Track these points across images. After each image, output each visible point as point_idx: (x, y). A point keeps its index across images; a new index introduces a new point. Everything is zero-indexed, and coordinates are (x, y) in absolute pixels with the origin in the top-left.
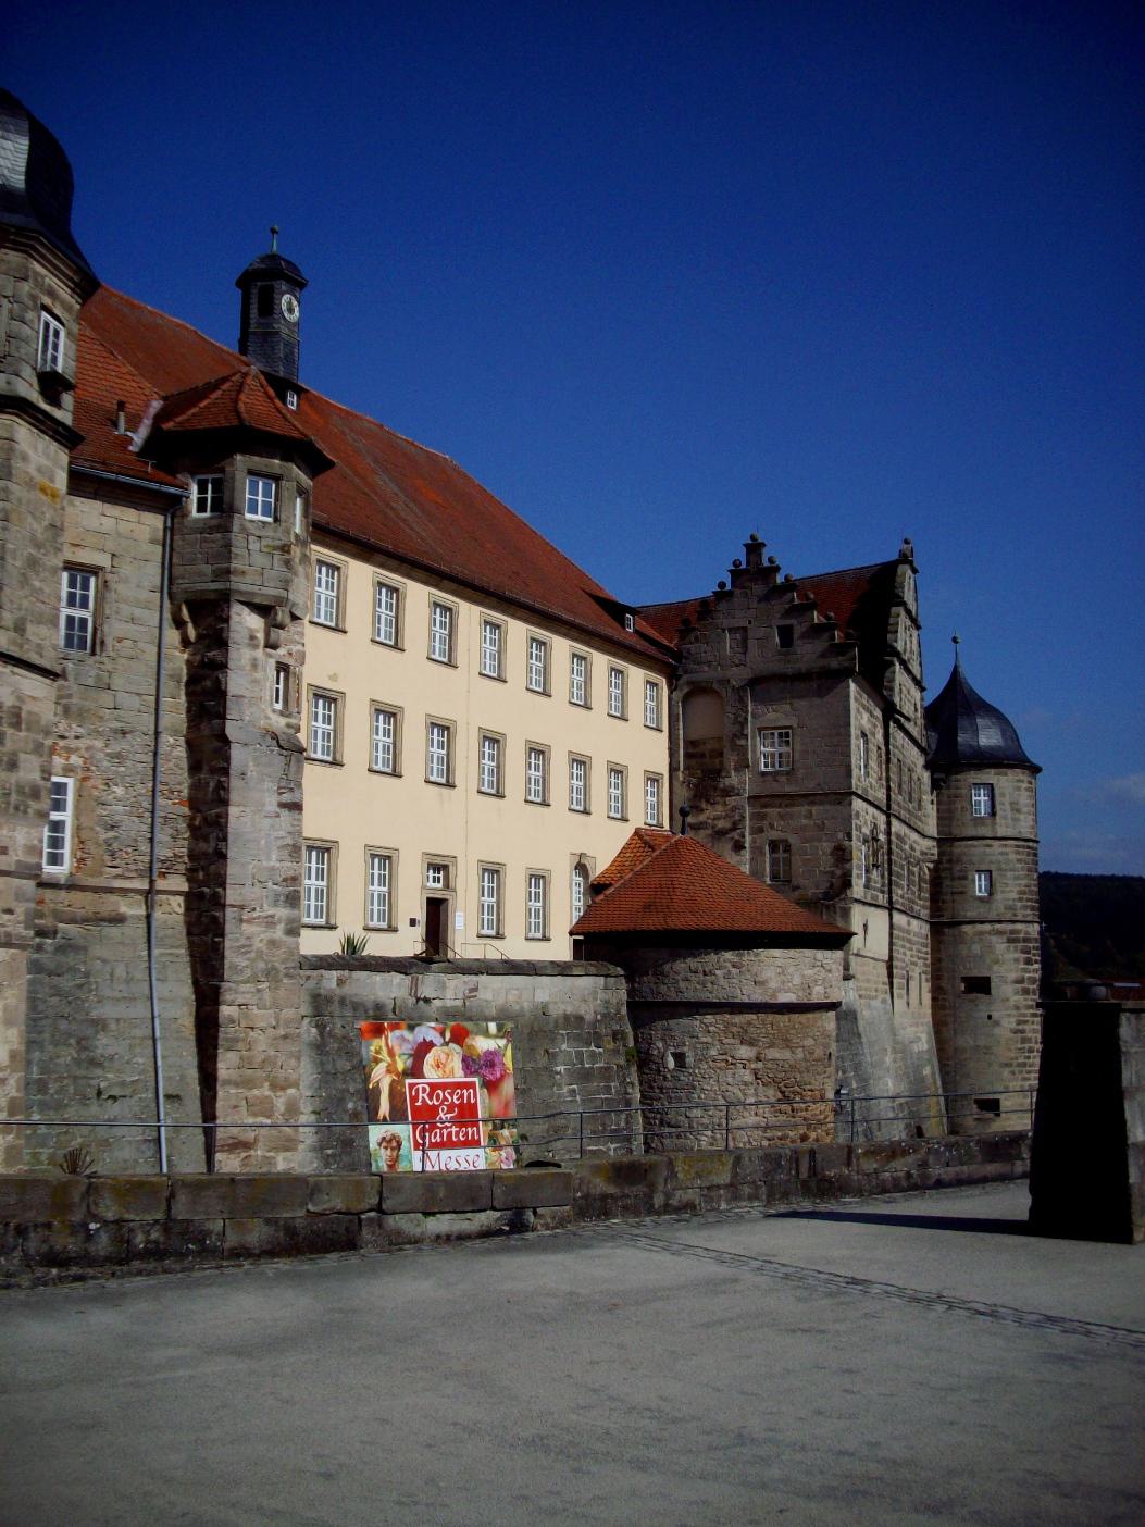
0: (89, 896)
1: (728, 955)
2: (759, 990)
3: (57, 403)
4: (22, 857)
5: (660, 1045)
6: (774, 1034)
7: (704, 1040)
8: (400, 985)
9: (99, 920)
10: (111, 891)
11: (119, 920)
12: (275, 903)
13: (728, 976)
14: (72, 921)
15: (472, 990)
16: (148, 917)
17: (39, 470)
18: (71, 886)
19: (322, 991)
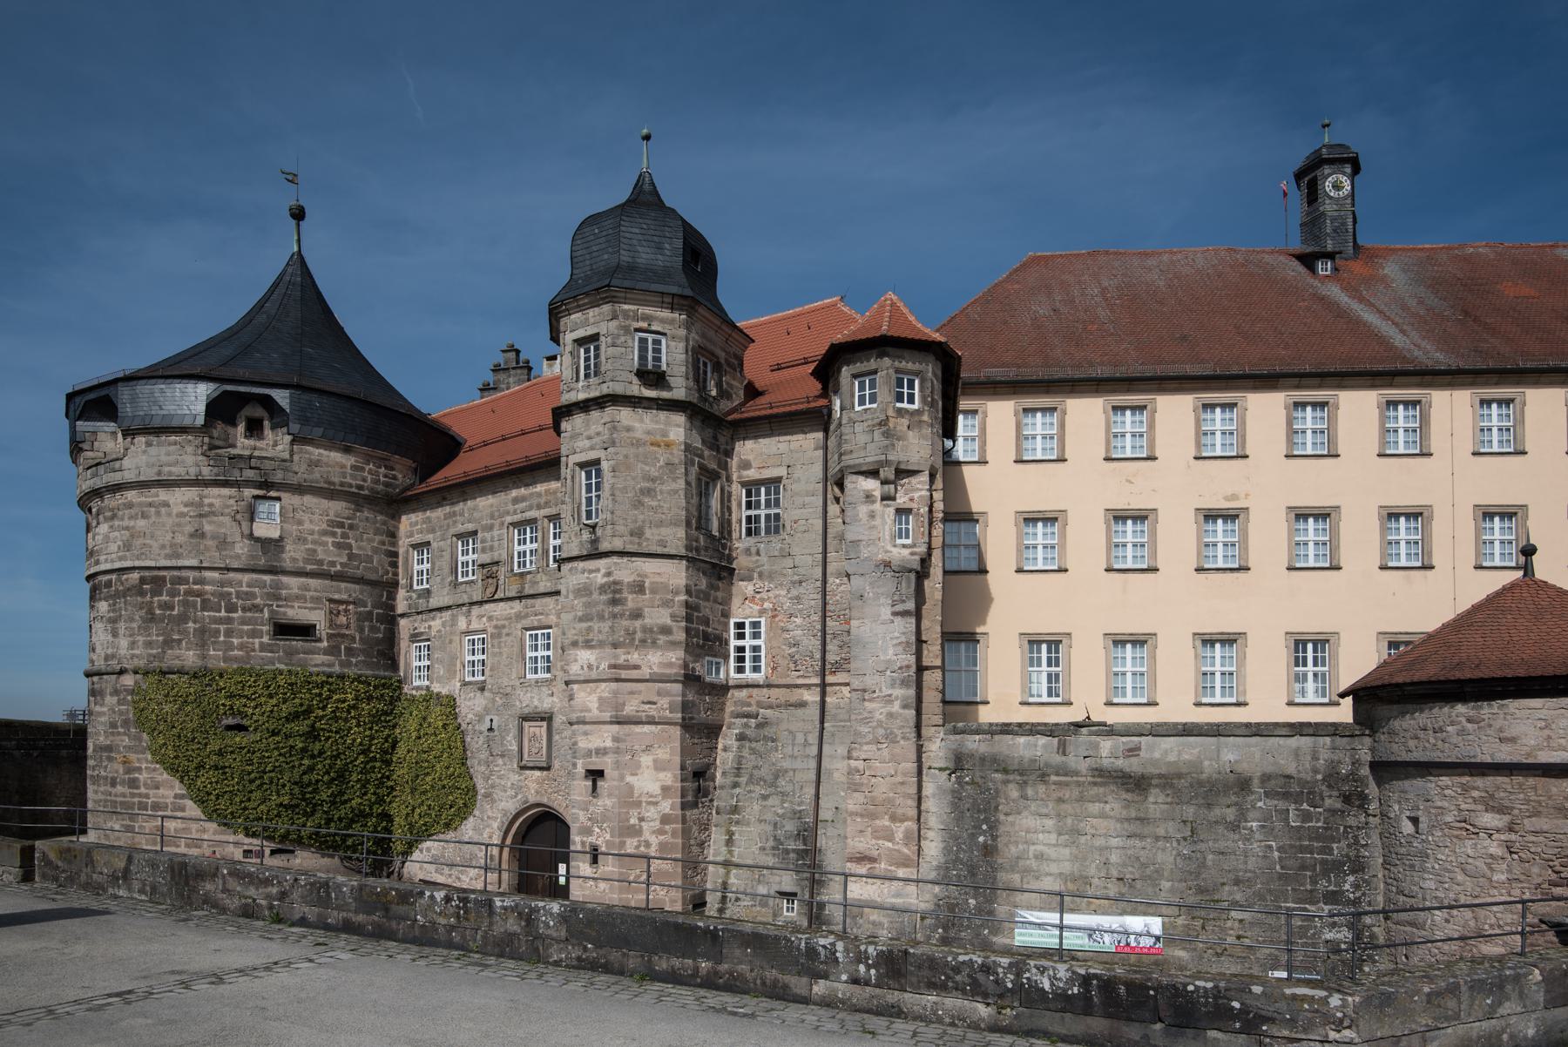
0: (783, 690)
1: (1461, 708)
2: (1506, 748)
3: (669, 388)
4: (656, 669)
5: (1396, 807)
6: (1539, 802)
7: (1439, 804)
8: (1045, 746)
9: (789, 705)
10: (797, 686)
11: (802, 704)
12: (893, 686)
13: (1462, 732)
14: (770, 707)
15: (1130, 750)
16: (823, 703)
17: (649, 433)
18: (769, 686)
19: (964, 750)
